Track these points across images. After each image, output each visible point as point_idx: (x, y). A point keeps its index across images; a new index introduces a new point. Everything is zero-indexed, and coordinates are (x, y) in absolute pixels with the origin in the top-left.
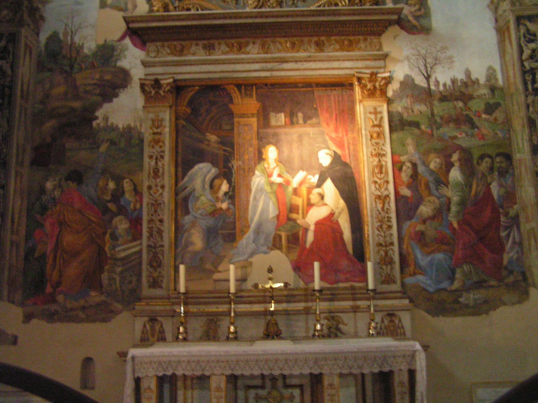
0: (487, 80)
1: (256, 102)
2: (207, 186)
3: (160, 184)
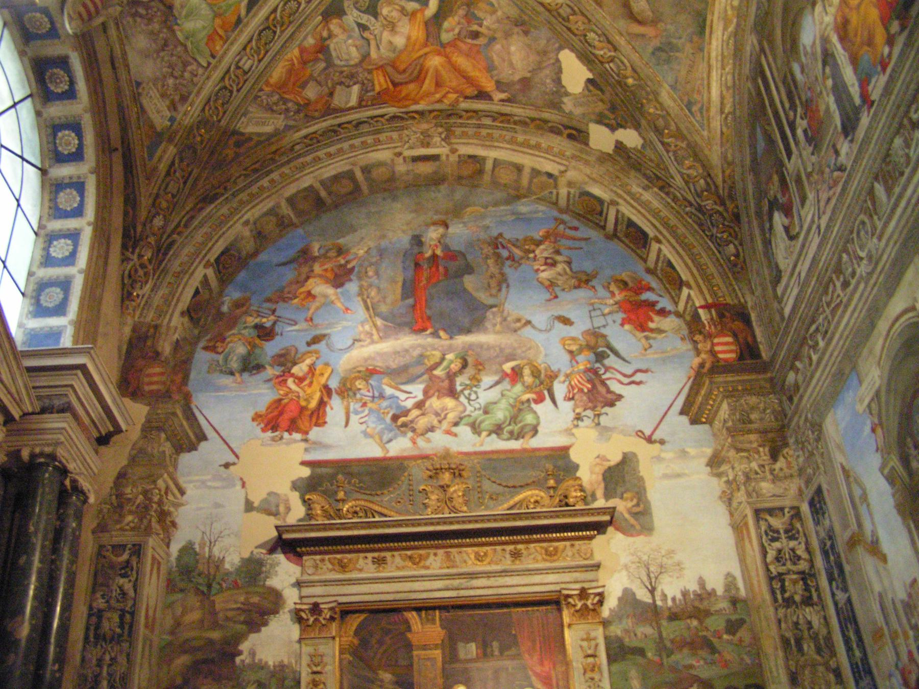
0: (726, 591)
1: (440, 629)
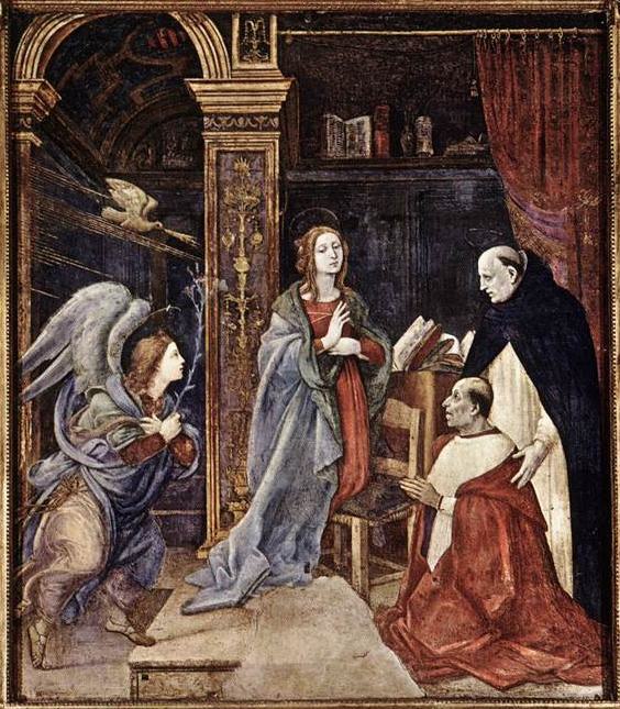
2: (113, 362)
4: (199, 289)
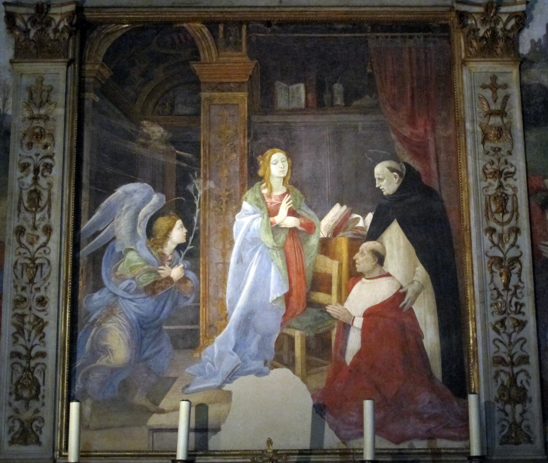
1: (246, 59)
2: (141, 231)
3: (43, 224)
4: (197, 188)
